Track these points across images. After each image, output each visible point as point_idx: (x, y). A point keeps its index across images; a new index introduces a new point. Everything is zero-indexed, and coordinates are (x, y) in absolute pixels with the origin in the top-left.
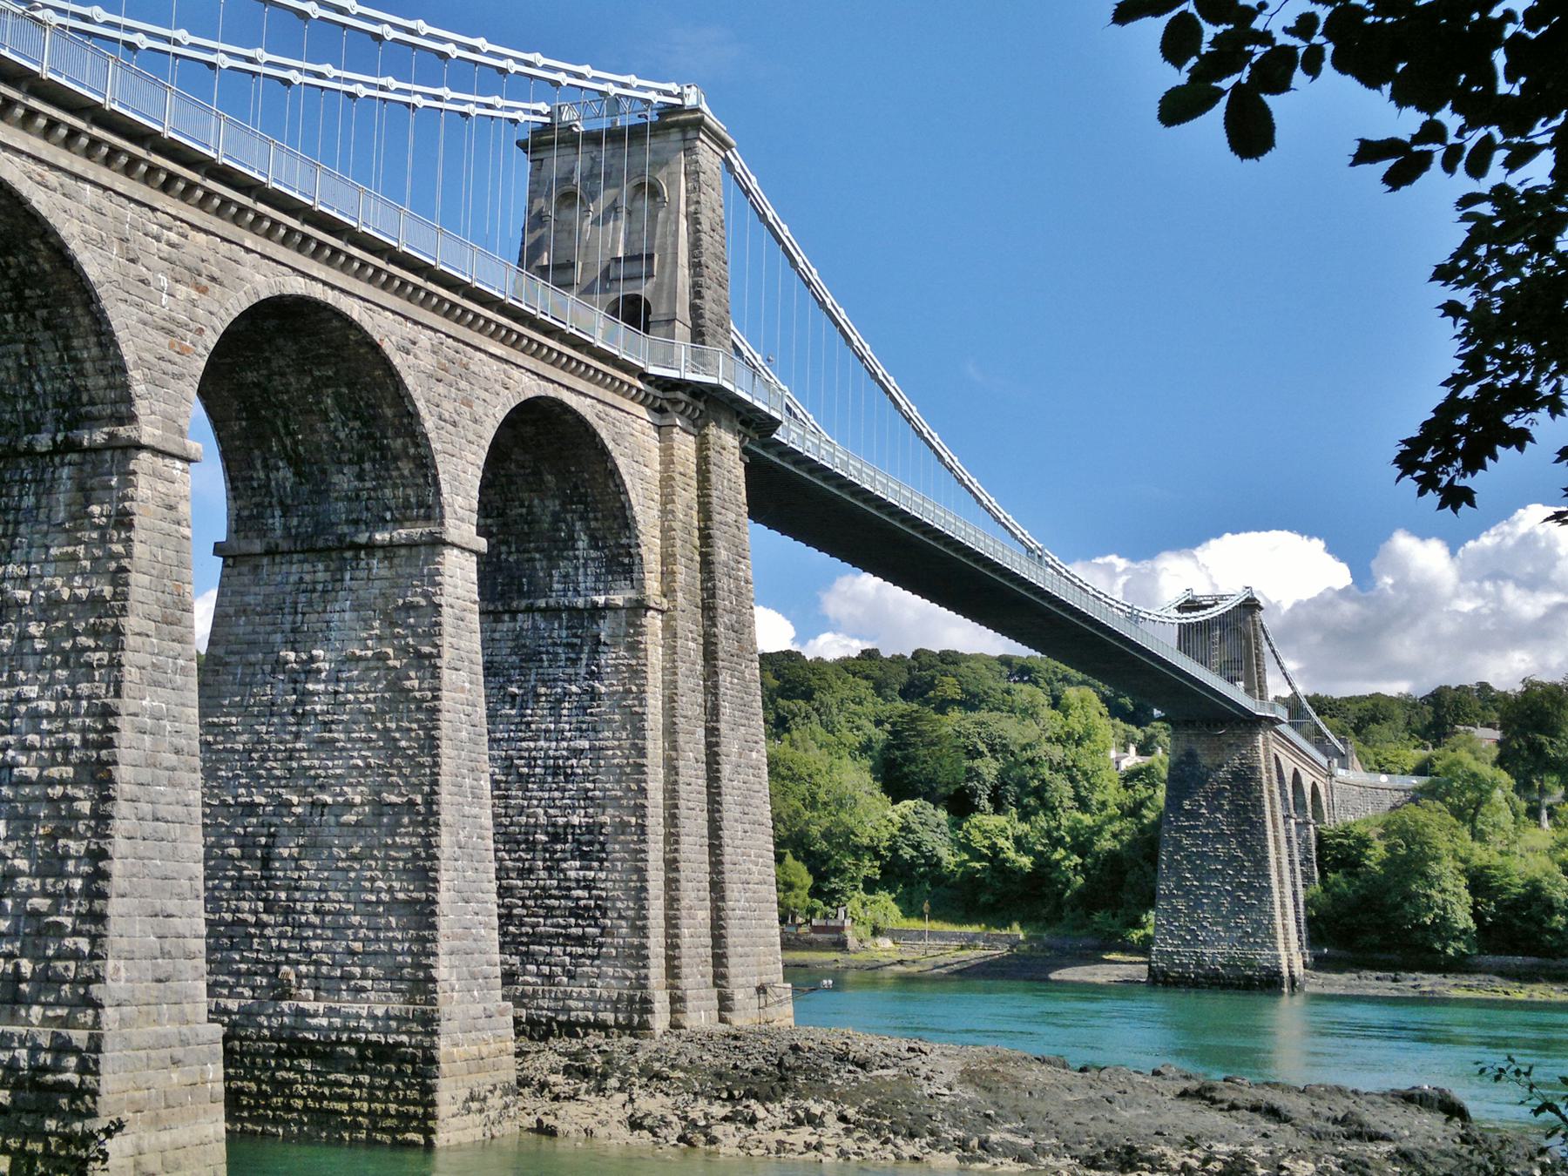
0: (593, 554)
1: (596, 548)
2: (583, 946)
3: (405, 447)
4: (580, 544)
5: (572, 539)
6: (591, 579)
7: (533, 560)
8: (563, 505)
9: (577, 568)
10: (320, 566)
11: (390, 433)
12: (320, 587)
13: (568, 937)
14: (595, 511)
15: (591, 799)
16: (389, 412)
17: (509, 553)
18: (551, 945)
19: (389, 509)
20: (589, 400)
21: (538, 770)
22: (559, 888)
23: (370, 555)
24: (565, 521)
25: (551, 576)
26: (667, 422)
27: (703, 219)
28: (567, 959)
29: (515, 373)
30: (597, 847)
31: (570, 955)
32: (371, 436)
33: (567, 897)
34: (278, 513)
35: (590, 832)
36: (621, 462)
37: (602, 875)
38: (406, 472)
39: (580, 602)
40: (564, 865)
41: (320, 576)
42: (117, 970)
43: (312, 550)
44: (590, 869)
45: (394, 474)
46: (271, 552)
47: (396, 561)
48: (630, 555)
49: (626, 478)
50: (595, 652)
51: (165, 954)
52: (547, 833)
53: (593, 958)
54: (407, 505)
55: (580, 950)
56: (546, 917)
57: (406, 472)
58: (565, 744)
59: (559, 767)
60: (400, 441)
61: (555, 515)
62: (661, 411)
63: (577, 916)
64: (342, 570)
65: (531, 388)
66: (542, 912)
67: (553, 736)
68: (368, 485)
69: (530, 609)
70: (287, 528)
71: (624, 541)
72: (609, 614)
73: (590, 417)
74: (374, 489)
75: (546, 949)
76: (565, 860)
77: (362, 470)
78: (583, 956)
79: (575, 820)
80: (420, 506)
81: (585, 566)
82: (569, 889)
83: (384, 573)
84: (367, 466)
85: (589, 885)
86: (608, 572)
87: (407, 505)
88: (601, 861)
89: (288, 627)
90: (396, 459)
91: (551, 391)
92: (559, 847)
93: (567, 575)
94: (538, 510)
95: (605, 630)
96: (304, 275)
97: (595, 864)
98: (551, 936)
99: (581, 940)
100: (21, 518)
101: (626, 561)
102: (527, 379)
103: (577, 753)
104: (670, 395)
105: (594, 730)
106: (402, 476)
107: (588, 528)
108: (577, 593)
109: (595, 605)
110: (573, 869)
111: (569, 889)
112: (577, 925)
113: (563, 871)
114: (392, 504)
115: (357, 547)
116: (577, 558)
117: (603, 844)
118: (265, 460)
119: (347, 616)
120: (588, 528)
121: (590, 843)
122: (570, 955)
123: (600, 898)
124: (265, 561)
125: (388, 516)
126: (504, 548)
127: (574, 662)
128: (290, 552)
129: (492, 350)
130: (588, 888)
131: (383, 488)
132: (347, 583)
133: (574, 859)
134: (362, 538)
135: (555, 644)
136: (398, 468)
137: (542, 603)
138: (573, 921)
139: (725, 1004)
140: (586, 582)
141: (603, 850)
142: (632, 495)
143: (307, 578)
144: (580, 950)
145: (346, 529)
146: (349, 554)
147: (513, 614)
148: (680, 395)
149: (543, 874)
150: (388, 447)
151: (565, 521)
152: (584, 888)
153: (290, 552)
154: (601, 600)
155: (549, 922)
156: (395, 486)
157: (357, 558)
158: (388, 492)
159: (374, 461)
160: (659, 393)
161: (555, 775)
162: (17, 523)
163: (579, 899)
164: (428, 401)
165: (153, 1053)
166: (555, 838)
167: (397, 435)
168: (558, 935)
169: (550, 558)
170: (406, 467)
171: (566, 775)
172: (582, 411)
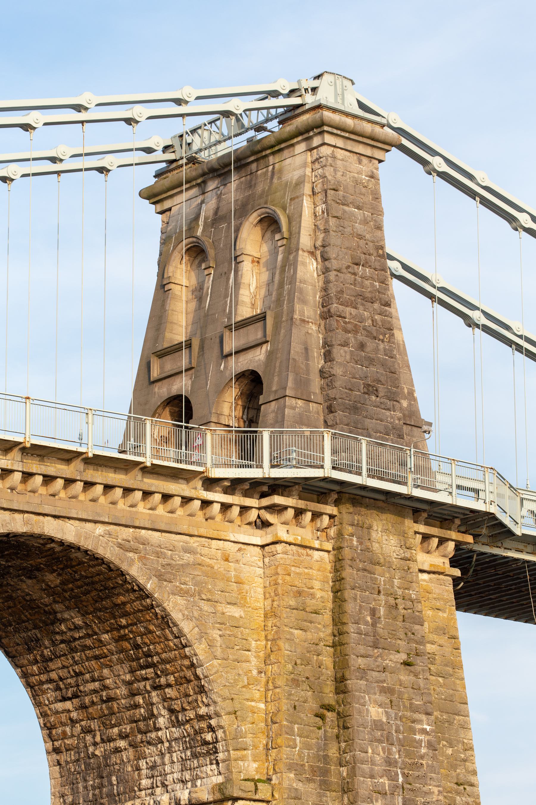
0: (176, 732)
1: (178, 724)
4: (162, 722)
6: (177, 767)
7: (117, 750)
9: (162, 755)
14: (166, 673)
17: (95, 744)
20: (100, 529)
36: (175, 606)
48: (211, 729)
49: (186, 627)
71: (203, 711)
73: (108, 551)
81: (170, 750)
86: (195, 756)
93: (153, 767)
104: (266, 502)
142: (200, 650)
148: (278, 499)
172: (88, 545)
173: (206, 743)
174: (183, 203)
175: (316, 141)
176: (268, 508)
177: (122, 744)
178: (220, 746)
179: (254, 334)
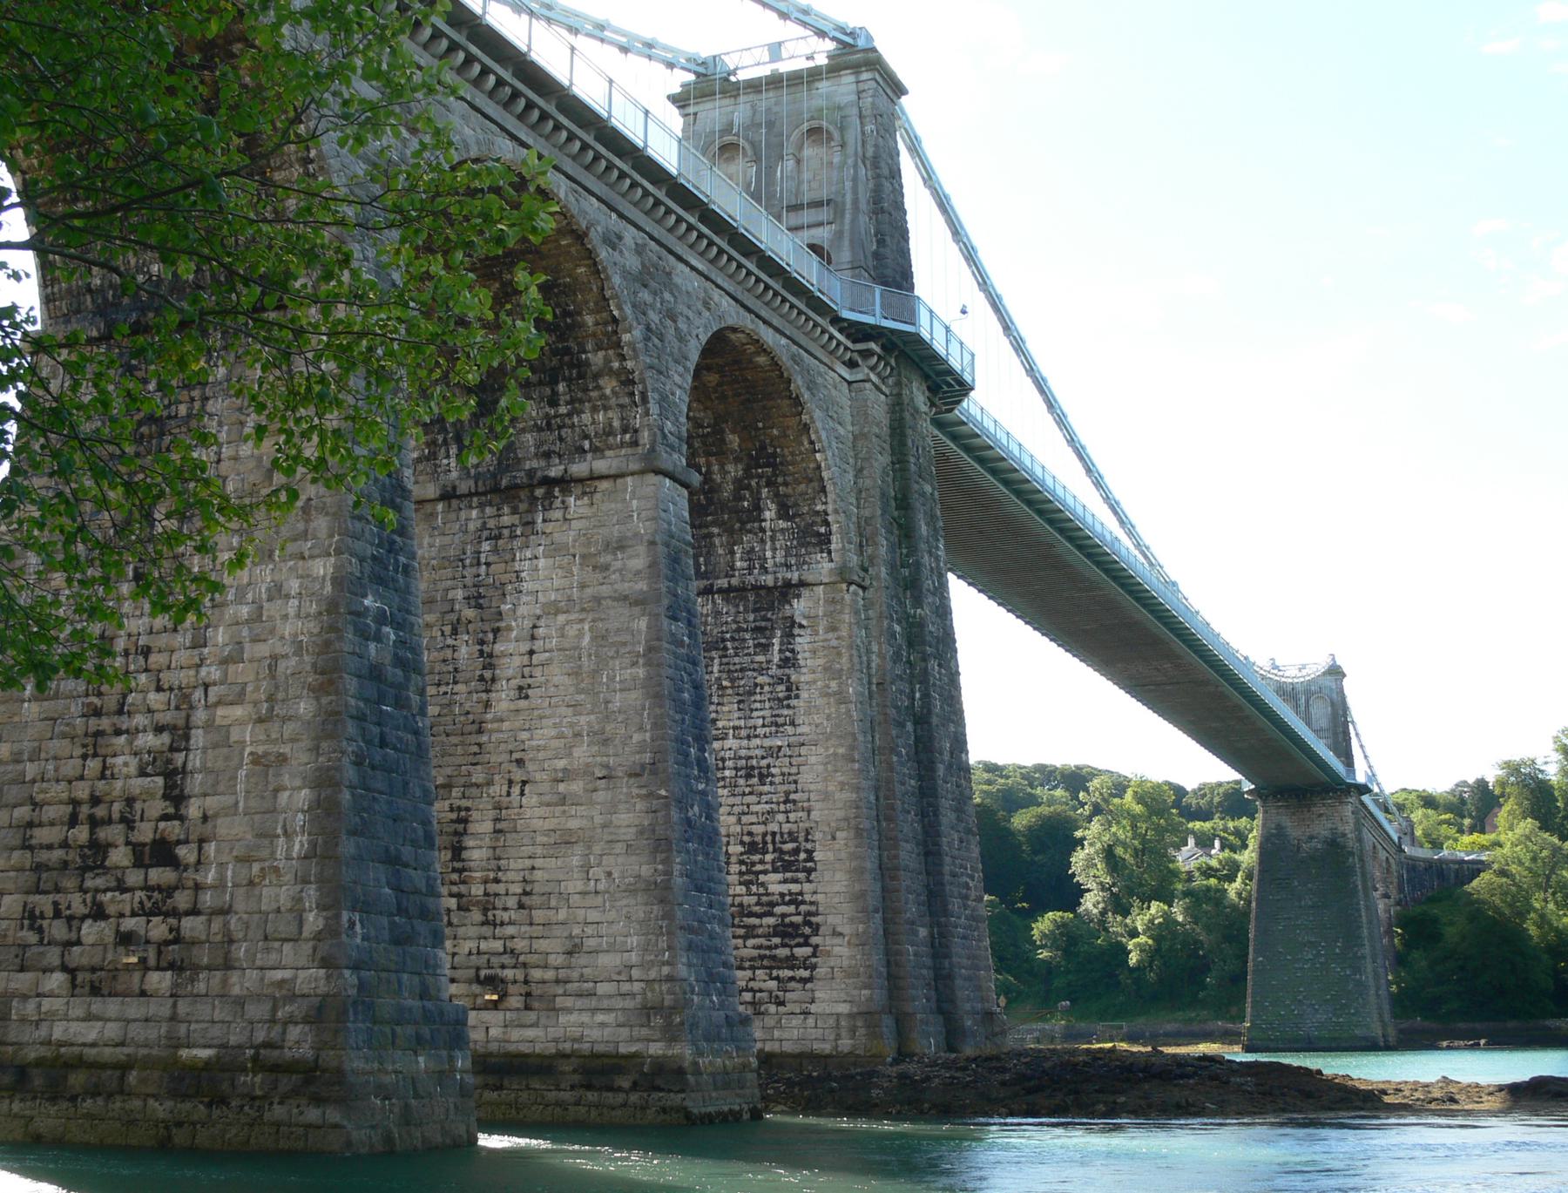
0: (782, 524)
2: (792, 968)
3: (607, 360)
4: (767, 515)
5: (758, 508)
6: (780, 554)
8: (747, 470)
9: (763, 541)
10: (506, 509)
11: (589, 347)
12: (506, 532)
13: (773, 958)
15: (794, 802)
16: (589, 320)
18: (753, 968)
19: (586, 437)
21: (727, 773)
22: (758, 904)
23: (566, 492)
24: (748, 487)
25: (732, 553)
26: (860, 377)
27: (883, 164)
28: (773, 984)
29: (716, 294)
30: (803, 856)
31: (777, 978)
32: (567, 351)
33: (771, 914)
34: (453, 450)
35: (795, 840)
37: (807, 887)
38: (608, 392)
39: (769, 580)
40: (762, 878)
41: (506, 520)
42: (352, 924)
43: (496, 490)
44: (795, 881)
45: (594, 394)
46: (448, 495)
47: (598, 496)
50: (789, 636)
51: (401, 911)
52: (742, 843)
53: (804, 981)
54: (609, 432)
55: (789, 973)
56: (745, 937)
57: (608, 392)
58: (758, 741)
59: (753, 768)
60: (601, 354)
61: (737, 481)
62: (852, 364)
63: (783, 935)
64: (531, 510)
65: (733, 315)
66: (742, 932)
67: (743, 733)
68: (563, 410)
70: (464, 469)
71: (819, 507)
72: (805, 592)
74: (569, 415)
75: (749, 973)
76: (765, 872)
77: (555, 393)
78: (792, 979)
79: (773, 827)
80: (625, 431)
81: (773, 539)
82: (772, 904)
83: (586, 511)
84: (561, 387)
85: (795, 900)
86: (801, 545)
87: (609, 432)
88: (809, 871)
89: (469, 581)
90: (596, 376)
91: (747, 321)
92: (757, 858)
94: (718, 478)
95: (800, 607)
96: (513, 137)
97: (801, 875)
98: (752, 959)
99: (791, 962)
100: (208, 392)
101: (823, 530)
102: (726, 302)
103: (774, 752)
104: (860, 346)
105: (793, 724)
106: (603, 397)
107: (777, 495)
108: (765, 570)
109: (788, 584)
110: (775, 884)
111: (772, 904)
112: (784, 945)
113: (763, 884)
114: (591, 430)
115: (548, 482)
116: (763, 530)
117: (810, 852)
119: (542, 563)
120: (777, 495)
121: (796, 851)
122: (777, 978)
123: (809, 914)
124: (440, 507)
125: (587, 445)
127: (765, 648)
128: (470, 495)
129: (694, 262)
130: (797, 904)
132: (540, 525)
133: (775, 871)
135: (739, 630)
136: (598, 388)
137: (722, 583)
138: (777, 940)
139: (952, 1036)
140: (773, 556)
141: (810, 859)
143: (491, 523)
144: (789, 973)
145: (535, 464)
146: (539, 492)
148: (873, 346)
149: (741, 889)
150: (587, 363)
151: (748, 487)
152: (788, 904)
153: (470, 495)
154: (794, 576)
155: (750, 942)
156: (595, 410)
157: (549, 496)
158: (586, 417)
159: (569, 380)
160: (850, 344)
161: (749, 776)
162: (205, 399)
163: (784, 916)
164: (634, 306)
165: (398, 1029)
166: (752, 848)
167: (599, 348)
168: (762, 957)
169: (730, 532)
170: (609, 385)
171: (762, 777)
173: (819, 534)
174: (713, 113)
175: (865, 76)
176: (859, 352)
177: (716, 530)
178: (834, 538)
179: (824, 214)
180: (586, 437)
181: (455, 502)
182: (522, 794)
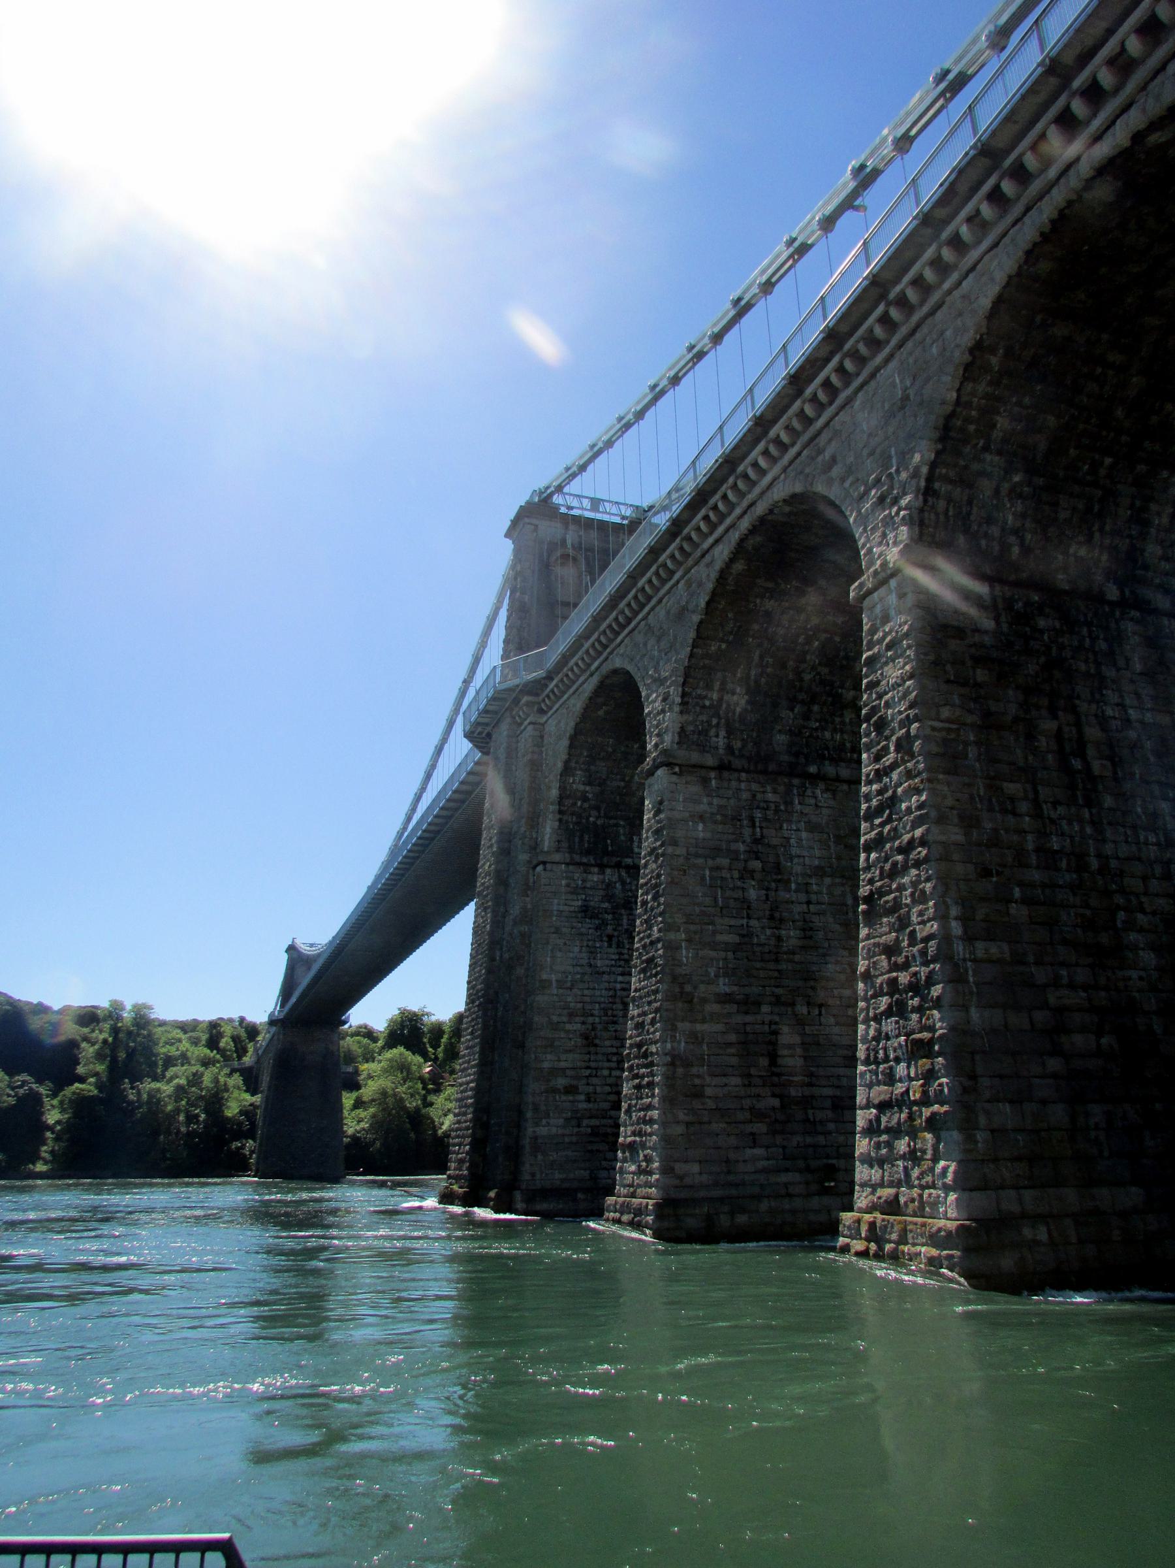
7: (617, 825)
10: (769, 788)
17: (598, 818)
34: (722, 733)
38: (847, 720)
43: (765, 772)
45: (837, 720)
57: (847, 720)
69: (618, 865)
106: (843, 723)
118: (723, 683)
124: (713, 774)
126: (594, 813)
131: (823, 729)
134: (813, 769)
147: (602, 867)
156: (835, 730)
158: (827, 735)
180: (827, 748)
181: (726, 774)
182: (820, 1014)
